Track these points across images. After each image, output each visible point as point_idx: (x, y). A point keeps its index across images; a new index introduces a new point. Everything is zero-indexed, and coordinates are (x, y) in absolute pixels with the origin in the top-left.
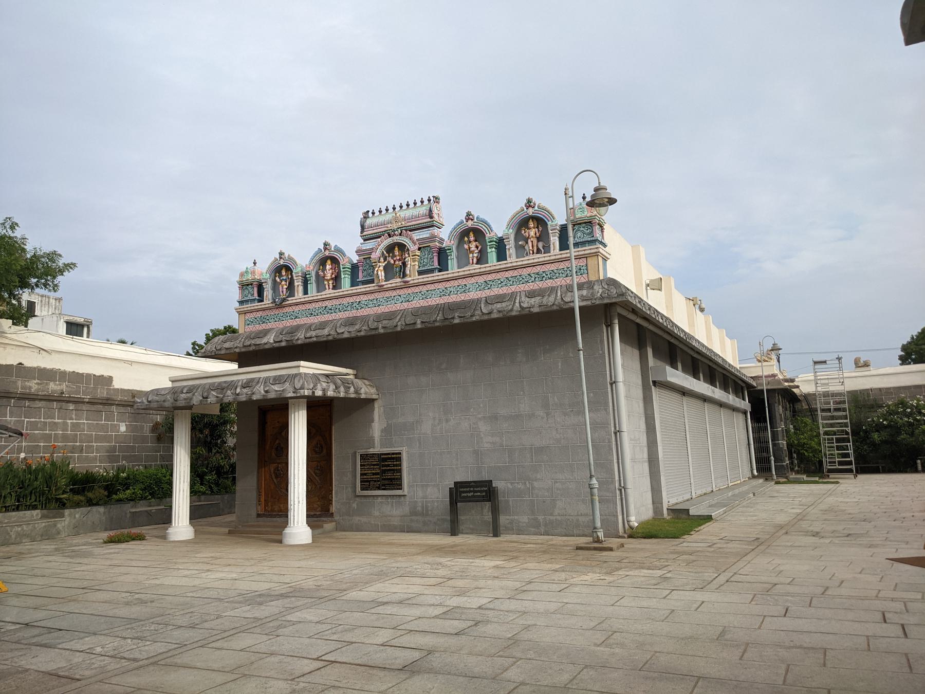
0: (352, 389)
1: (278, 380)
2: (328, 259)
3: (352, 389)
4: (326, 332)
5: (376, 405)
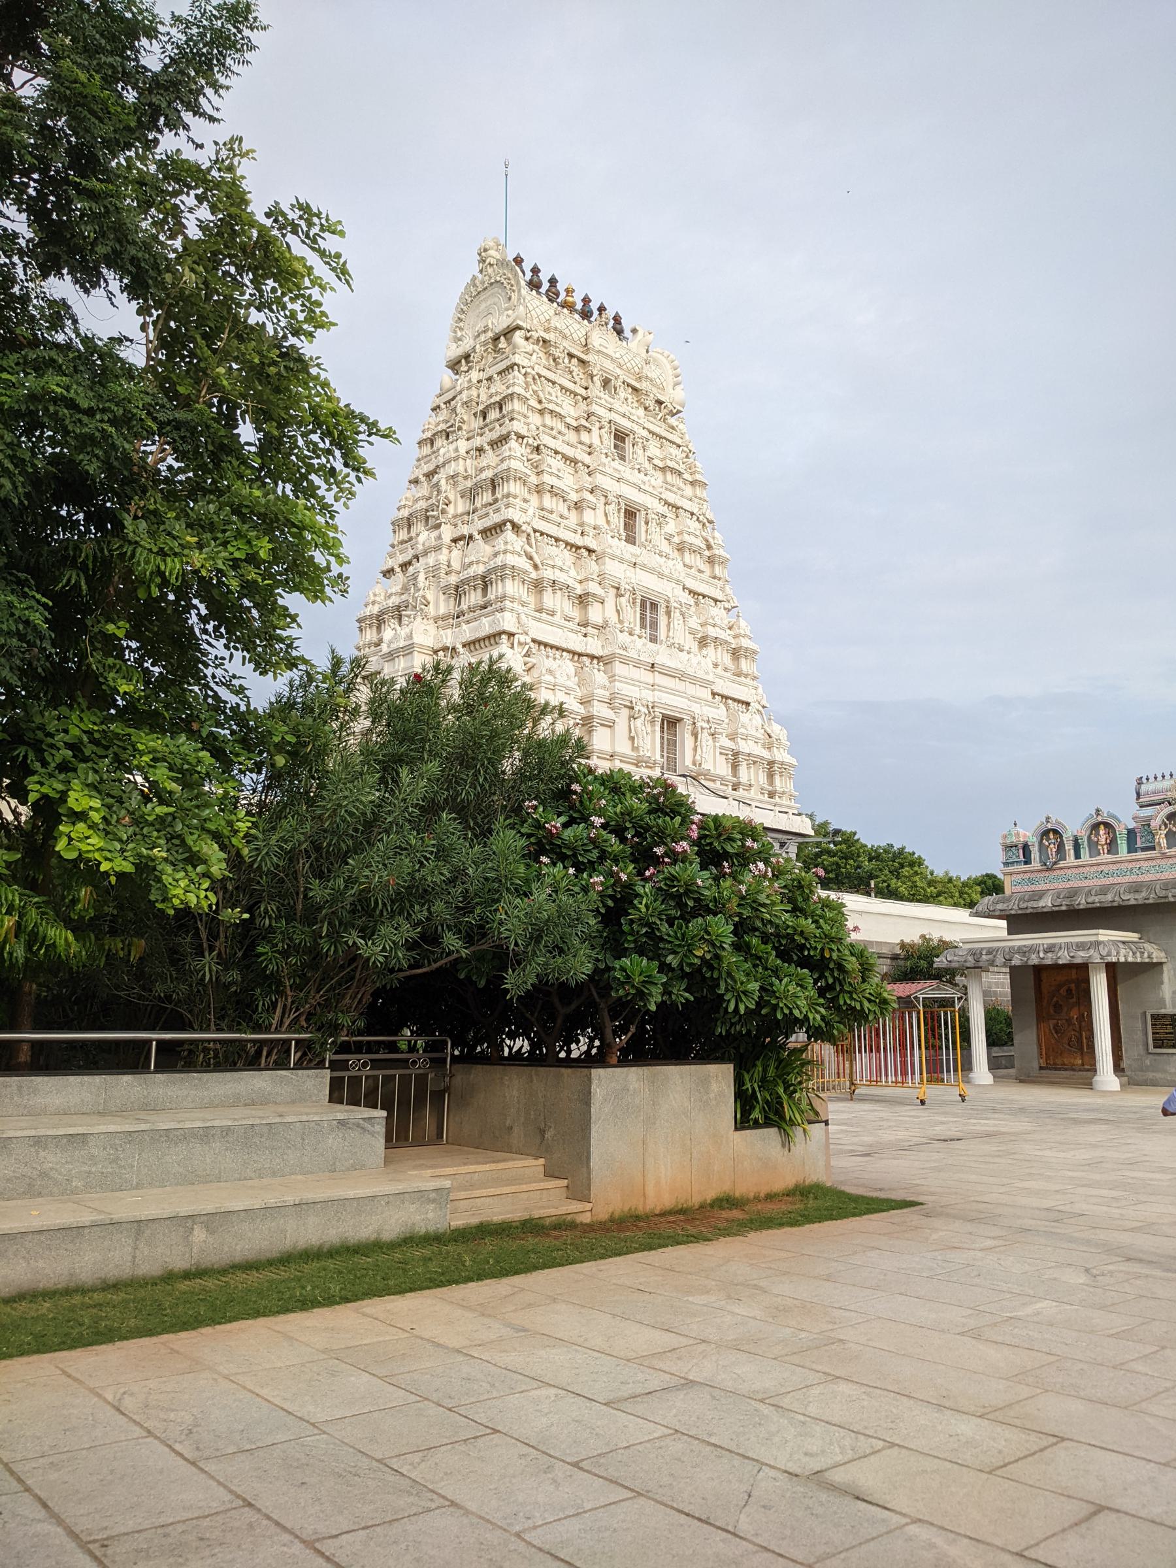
0: (1146, 955)
1: (1081, 946)
2: (1100, 824)
3: (1146, 955)
4: (1109, 897)
5: (1165, 968)
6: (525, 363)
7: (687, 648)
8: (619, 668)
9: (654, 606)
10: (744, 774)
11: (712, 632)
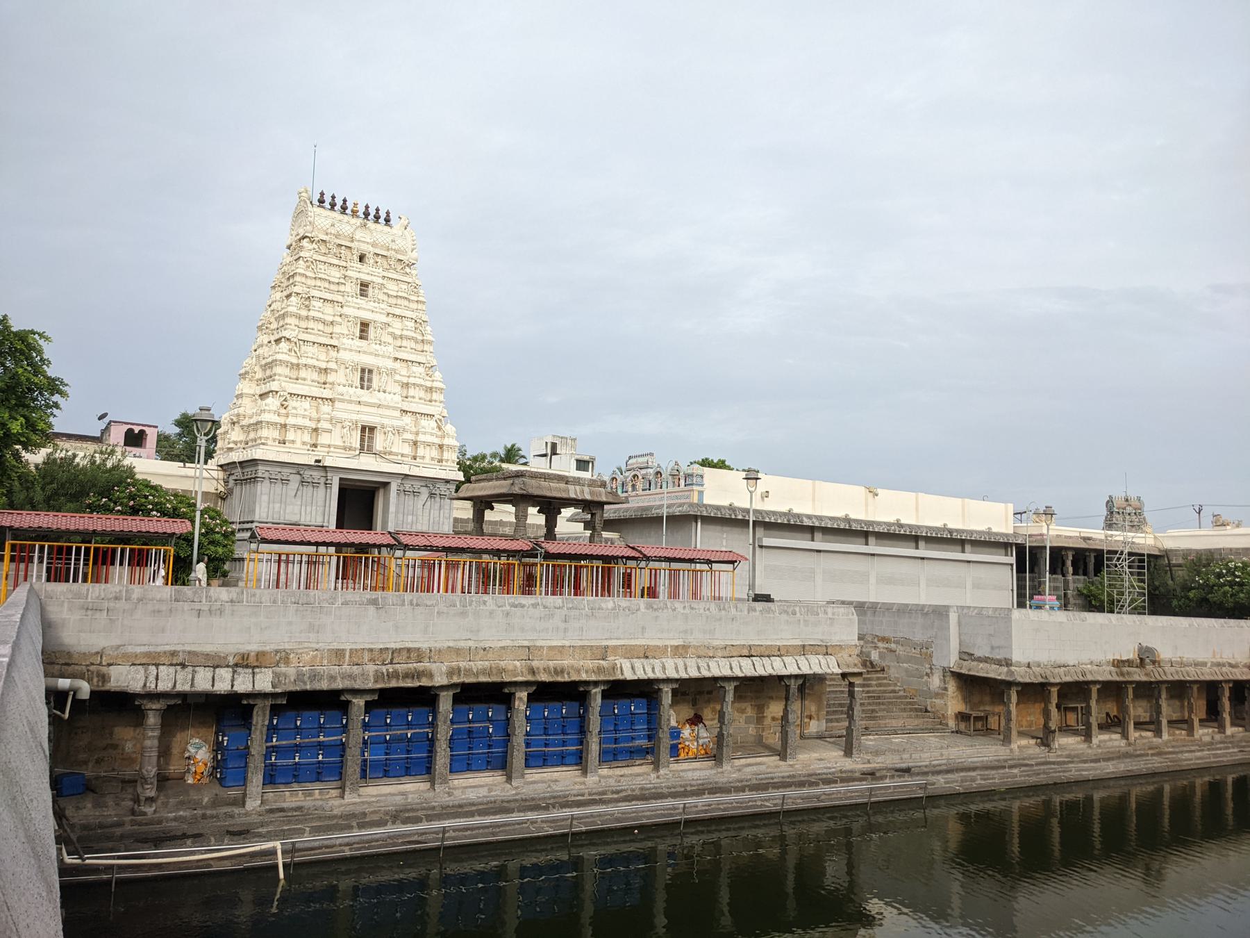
6: (307, 254)
7: (388, 390)
8: (337, 404)
9: (370, 371)
10: (421, 452)
11: (412, 380)
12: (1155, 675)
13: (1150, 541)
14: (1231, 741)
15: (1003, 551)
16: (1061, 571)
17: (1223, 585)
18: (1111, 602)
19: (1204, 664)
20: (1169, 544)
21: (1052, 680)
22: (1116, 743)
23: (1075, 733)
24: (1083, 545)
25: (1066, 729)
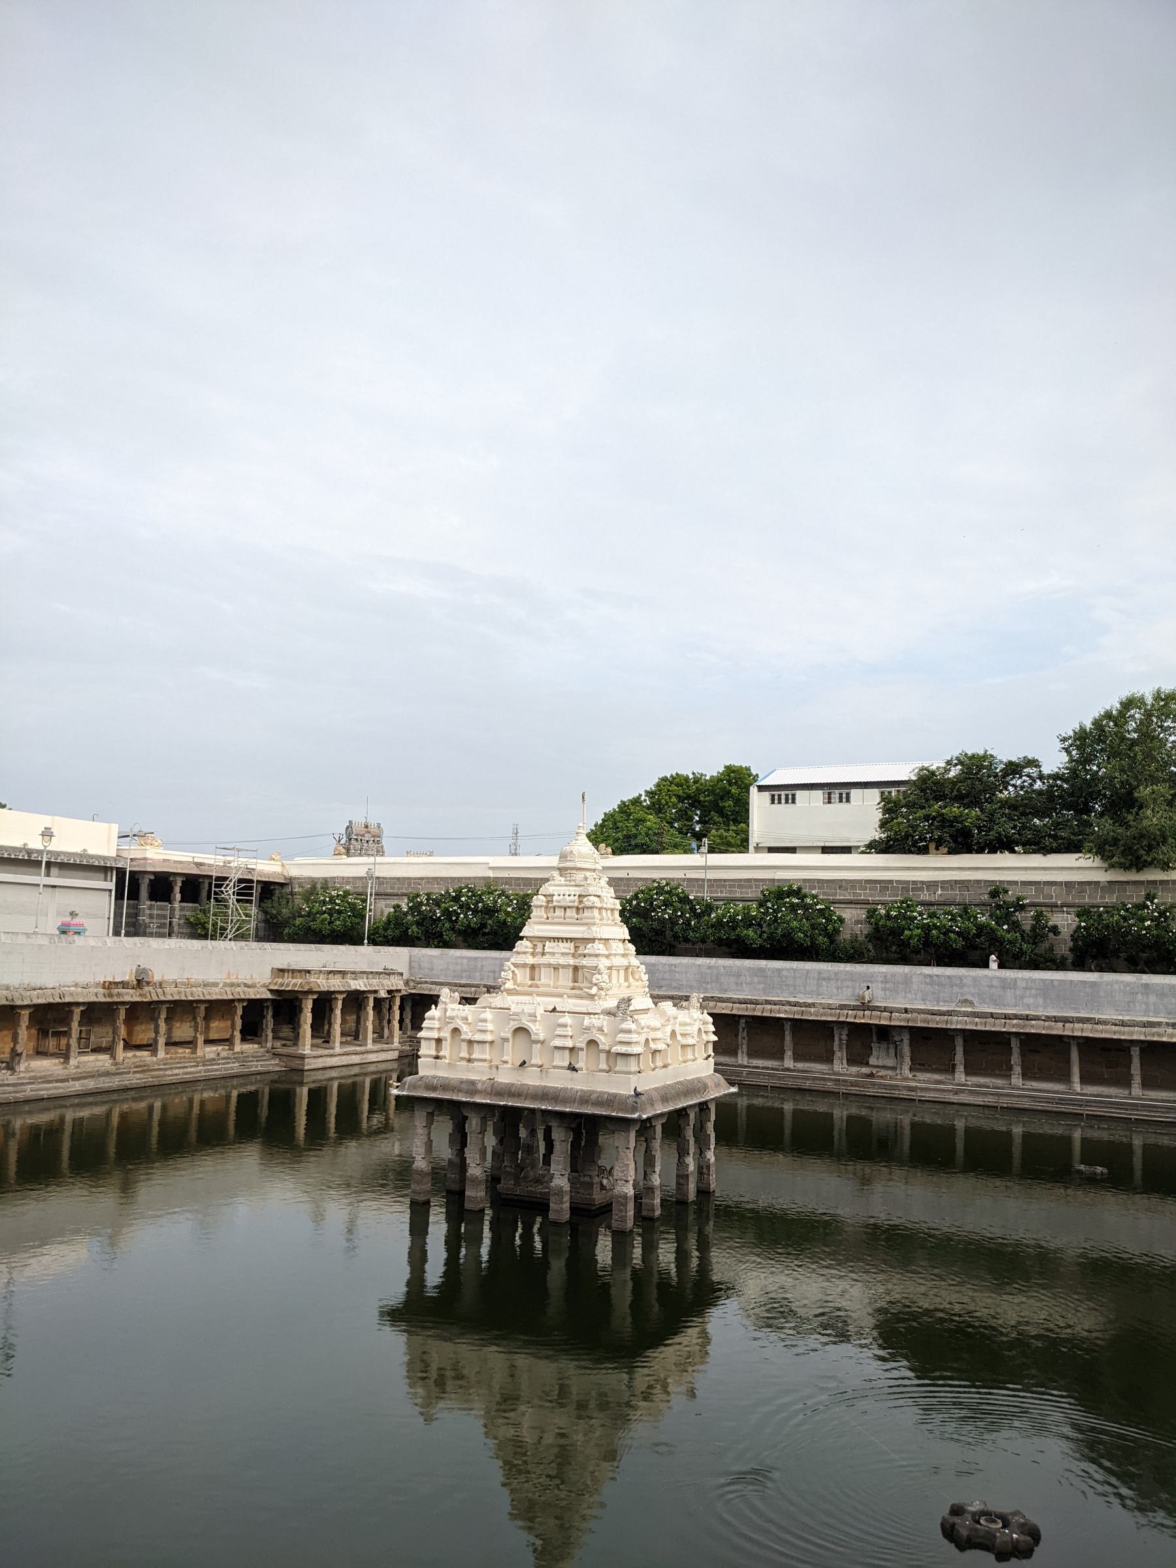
12: (150, 994)
13: (278, 869)
14: (242, 1058)
15: (102, 876)
16: (153, 896)
17: (325, 912)
18: (215, 930)
19: (215, 985)
20: (294, 872)
21: (19, 1003)
22: (101, 1064)
23: (54, 1055)
24: (195, 871)
25: (40, 1053)
